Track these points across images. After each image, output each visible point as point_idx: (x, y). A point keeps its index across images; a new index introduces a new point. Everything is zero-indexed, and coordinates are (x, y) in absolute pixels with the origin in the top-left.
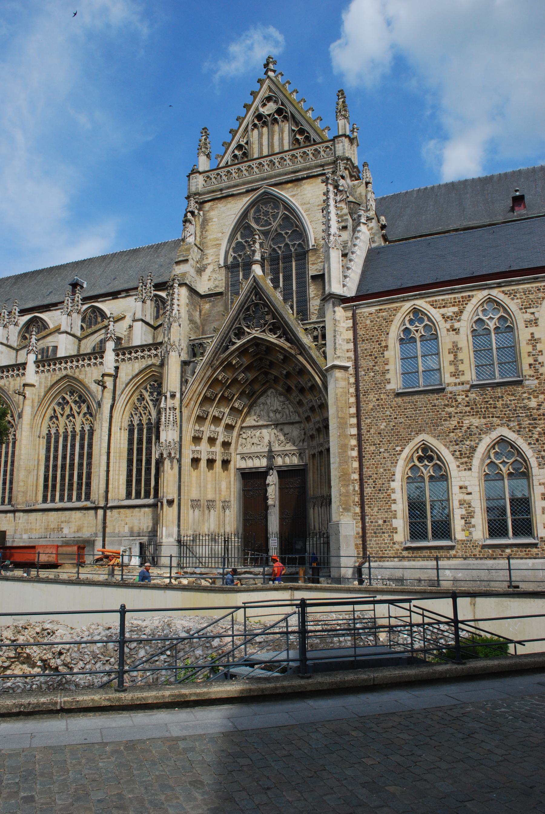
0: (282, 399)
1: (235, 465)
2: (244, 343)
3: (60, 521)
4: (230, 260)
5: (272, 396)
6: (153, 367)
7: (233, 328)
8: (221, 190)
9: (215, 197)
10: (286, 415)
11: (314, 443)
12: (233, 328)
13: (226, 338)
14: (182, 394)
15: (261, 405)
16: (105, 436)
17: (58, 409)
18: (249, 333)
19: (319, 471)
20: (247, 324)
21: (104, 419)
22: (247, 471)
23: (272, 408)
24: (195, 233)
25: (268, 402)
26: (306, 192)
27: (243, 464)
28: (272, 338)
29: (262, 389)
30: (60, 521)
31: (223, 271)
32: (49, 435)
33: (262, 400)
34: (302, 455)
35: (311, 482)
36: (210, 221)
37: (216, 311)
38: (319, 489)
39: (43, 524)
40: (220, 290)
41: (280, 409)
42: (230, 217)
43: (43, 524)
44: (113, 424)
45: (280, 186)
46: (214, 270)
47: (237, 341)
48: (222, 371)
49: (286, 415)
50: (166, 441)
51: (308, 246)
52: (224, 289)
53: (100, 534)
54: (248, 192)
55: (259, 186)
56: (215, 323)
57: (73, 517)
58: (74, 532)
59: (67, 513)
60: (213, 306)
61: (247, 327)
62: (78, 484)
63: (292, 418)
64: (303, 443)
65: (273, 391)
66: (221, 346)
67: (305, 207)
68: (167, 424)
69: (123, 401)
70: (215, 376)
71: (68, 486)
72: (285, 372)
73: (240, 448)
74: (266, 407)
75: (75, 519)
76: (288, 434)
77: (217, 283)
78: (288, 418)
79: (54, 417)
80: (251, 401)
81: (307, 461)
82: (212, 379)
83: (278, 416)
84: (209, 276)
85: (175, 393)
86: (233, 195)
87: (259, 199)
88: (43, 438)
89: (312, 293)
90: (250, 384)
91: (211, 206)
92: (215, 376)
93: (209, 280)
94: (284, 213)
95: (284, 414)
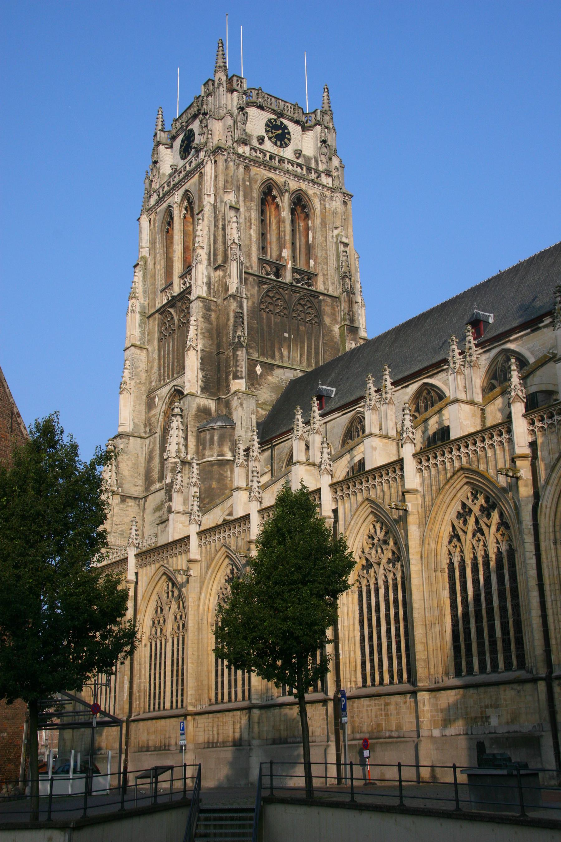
3: (483, 704)
16: (530, 558)
17: (459, 524)
21: (526, 531)
30: (483, 704)
32: (451, 565)
39: (460, 711)
43: (460, 711)
44: (542, 537)
53: (547, 727)
57: (502, 697)
58: (508, 723)
59: (492, 690)
62: (504, 641)
69: (551, 496)
71: (490, 645)
75: (505, 700)
79: (455, 536)
88: (442, 571)
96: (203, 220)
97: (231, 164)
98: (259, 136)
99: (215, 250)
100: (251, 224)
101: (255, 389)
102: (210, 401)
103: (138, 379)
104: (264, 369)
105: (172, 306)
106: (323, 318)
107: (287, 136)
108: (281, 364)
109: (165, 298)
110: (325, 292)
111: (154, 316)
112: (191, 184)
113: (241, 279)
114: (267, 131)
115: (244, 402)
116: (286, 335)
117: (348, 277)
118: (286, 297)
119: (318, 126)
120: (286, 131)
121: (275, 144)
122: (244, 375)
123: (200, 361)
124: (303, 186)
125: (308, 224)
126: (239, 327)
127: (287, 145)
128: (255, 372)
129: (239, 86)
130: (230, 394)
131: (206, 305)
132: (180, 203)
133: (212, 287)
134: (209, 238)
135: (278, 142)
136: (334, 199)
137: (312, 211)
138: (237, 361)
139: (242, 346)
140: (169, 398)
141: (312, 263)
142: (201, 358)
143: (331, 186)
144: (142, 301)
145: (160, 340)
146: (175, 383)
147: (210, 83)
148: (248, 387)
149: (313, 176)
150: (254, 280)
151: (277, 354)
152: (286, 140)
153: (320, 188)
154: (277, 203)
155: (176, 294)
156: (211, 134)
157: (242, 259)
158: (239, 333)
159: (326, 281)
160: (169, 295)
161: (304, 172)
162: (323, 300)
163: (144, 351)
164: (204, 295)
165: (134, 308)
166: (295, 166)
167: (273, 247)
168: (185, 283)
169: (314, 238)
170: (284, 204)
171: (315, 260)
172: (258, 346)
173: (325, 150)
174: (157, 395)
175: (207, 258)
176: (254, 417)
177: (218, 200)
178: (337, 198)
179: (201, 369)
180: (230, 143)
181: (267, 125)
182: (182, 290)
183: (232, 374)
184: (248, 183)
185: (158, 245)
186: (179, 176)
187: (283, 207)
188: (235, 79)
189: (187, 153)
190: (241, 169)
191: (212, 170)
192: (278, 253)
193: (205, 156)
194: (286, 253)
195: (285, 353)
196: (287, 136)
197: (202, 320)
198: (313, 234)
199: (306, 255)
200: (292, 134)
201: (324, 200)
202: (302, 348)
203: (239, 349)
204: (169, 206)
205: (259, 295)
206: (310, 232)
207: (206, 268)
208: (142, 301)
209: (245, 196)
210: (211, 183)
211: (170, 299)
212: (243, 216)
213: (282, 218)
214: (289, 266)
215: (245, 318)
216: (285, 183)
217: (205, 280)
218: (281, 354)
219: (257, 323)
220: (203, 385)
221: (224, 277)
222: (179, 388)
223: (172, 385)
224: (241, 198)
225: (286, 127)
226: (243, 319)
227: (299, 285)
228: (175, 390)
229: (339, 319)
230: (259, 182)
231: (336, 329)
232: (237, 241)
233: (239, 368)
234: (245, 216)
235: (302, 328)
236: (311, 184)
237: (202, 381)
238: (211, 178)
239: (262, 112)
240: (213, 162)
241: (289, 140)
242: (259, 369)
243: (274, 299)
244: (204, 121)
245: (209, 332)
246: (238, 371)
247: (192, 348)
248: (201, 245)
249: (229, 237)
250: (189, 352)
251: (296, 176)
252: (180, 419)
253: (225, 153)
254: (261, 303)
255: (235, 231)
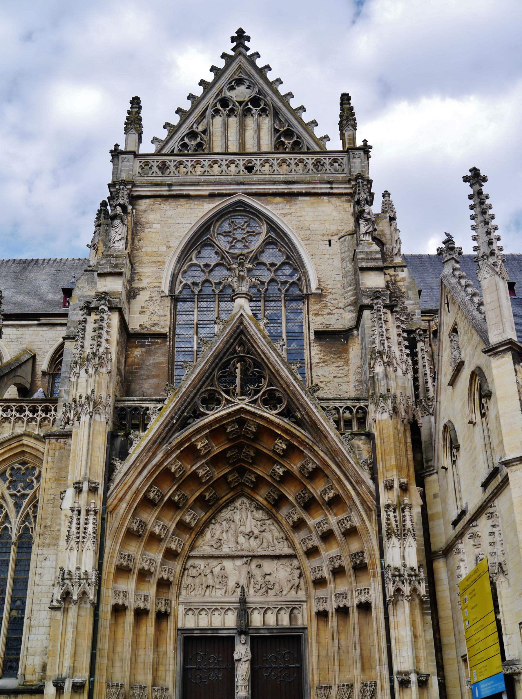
0: (260, 514)
1: (176, 623)
2: (222, 416)
4: (178, 289)
5: (244, 510)
6: (25, 438)
7: (203, 389)
8: (170, 185)
9: (158, 193)
10: (268, 542)
11: (321, 592)
12: (203, 389)
13: (189, 403)
14: (107, 488)
15: (224, 523)
18: (228, 402)
19: (336, 641)
20: (225, 387)
22: (197, 634)
23: (242, 529)
24: (127, 239)
25: (237, 517)
26: (304, 214)
27: (190, 622)
28: (271, 415)
29: (229, 496)
31: (168, 303)
33: (225, 514)
34: (296, 611)
35: (315, 659)
36: (147, 226)
37: (152, 361)
38: (337, 673)
40: (162, 331)
41: (256, 532)
42: (181, 226)
45: (263, 198)
46: (151, 299)
47: (207, 412)
48: (178, 457)
49: (268, 542)
50: (78, 569)
51: (308, 287)
52: (168, 330)
54: (212, 196)
55: (232, 192)
56: (150, 381)
60: (148, 353)
61: (225, 391)
63: (277, 547)
64: (297, 592)
65: (245, 500)
66: (180, 416)
67: (302, 233)
68: (81, 539)
70: (165, 464)
72: (281, 471)
73: (184, 592)
74: (233, 526)
76: (270, 574)
77: (155, 318)
78: (272, 549)
80: (208, 514)
81: (306, 623)
82: (161, 468)
83: (253, 543)
84: (143, 307)
85: (98, 485)
86: (187, 197)
87: (230, 209)
89: (316, 356)
90: (212, 486)
91: (150, 205)
92: (165, 464)
93: (141, 313)
94: (270, 236)
95: (265, 541)
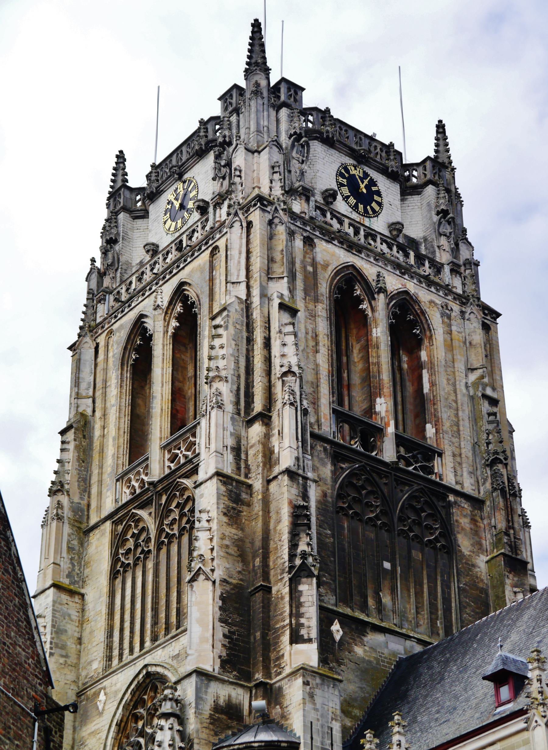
96: (226, 328)
97: (281, 229)
98: (327, 190)
99: (249, 385)
100: (317, 344)
101: (331, 669)
102: (240, 691)
103: (62, 656)
104: (346, 630)
105: (142, 507)
106: (456, 539)
107: (376, 197)
108: (376, 622)
109: (128, 491)
110: (458, 488)
111: (102, 527)
112: (192, 271)
113: (304, 441)
114: (341, 185)
115: (318, 692)
116: (387, 565)
117: (501, 462)
118: (385, 490)
119: (430, 186)
120: (374, 189)
121: (355, 208)
122: (314, 634)
123: (220, 603)
124: (412, 286)
125: (419, 358)
126: (303, 535)
127: (376, 214)
128: (330, 634)
129: (292, 99)
130: (284, 675)
131: (231, 491)
132: (168, 308)
133: (243, 456)
134: (237, 362)
135: (361, 207)
136: (467, 316)
137: (428, 333)
138: (299, 605)
139: (310, 575)
140: (133, 694)
141: (430, 430)
142: (222, 598)
143: (459, 291)
144: (76, 499)
145: (114, 575)
146: (148, 659)
147: (234, 93)
148: (323, 660)
149: (427, 269)
150: (325, 449)
151: (371, 602)
152: (374, 205)
153: (441, 293)
154: (363, 311)
155: (156, 479)
156: (240, 176)
157: (305, 403)
158: (302, 547)
159: (458, 469)
160: (136, 485)
161: (412, 260)
162: (455, 502)
163: (77, 599)
164: (228, 470)
165: (60, 511)
166: (395, 248)
167: (354, 394)
168: (172, 460)
169: (433, 384)
170: (377, 314)
171: (437, 424)
172: (334, 581)
173: (448, 229)
174: (104, 688)
175: (233, 399)
176: (337, 727)
177: (256, 292)
178: (472, 316)
179: (221, 620)
180: (278, 192)
181: (340, 174)
182: (167, 471)
183: (288, 632)
184: (310, 269)
185: (113, 391)
186: (165, 259)
187: (375, 320)
188: (283, 88)
189: (179, 222)
190: (299, 243)
191: (241, 238)
192: (365, 406)
193: (229, 214)
194: (384, 406)
195: (387, 600)
196: (376, 197)
197: (225, 519)
198: (431, 375)
199: (416, 416)
200: (383, 194)
201: (449, 317)
202: (419, 594)
203: (304, 580)
204: (142, 316)
205: (335, 480)
206: (425, 372)
207: (232, 418)
208: (76, 499)
209: (306, 291)
210: (239, 262)
211: (138, 491)
212: (302, 327)
213: (374, 339)
214: (391, 429)
215: (313, 519)
216: (378, 276)
217: (230, 442)
218: (379, 601)
219: (333, 536)
220: (224, 654)
221: (267, 436)
222: (159, 670)
223: (140, 664)
224: (299, 293)
225: (372, 183)
226: (309, 520)
227: (410, 468)
228: (148, 674)
229: (487, 540)
230: (330, 268)
231: (481, 561)
232: (295, 369)
233: (302, 620)
234: (306, 329)
235: (417, 555)
236: (424, 285)
237: (224, 645)
238: (240, 253)
239: (333, 151)
240: (245, 224)
241: (380, 204)
242: (336, 627)
243: (364, 492)
244: (224, 156)
245: (237, 546)
246: (303, 625)
247: (202, 577)
248: (223, 374)
249: (276, 362)
250: (195, 584)
251: (397, 266)
252: (177, 727)
253: (268, 209)
254: (340, 496)
255: (290, 350)
